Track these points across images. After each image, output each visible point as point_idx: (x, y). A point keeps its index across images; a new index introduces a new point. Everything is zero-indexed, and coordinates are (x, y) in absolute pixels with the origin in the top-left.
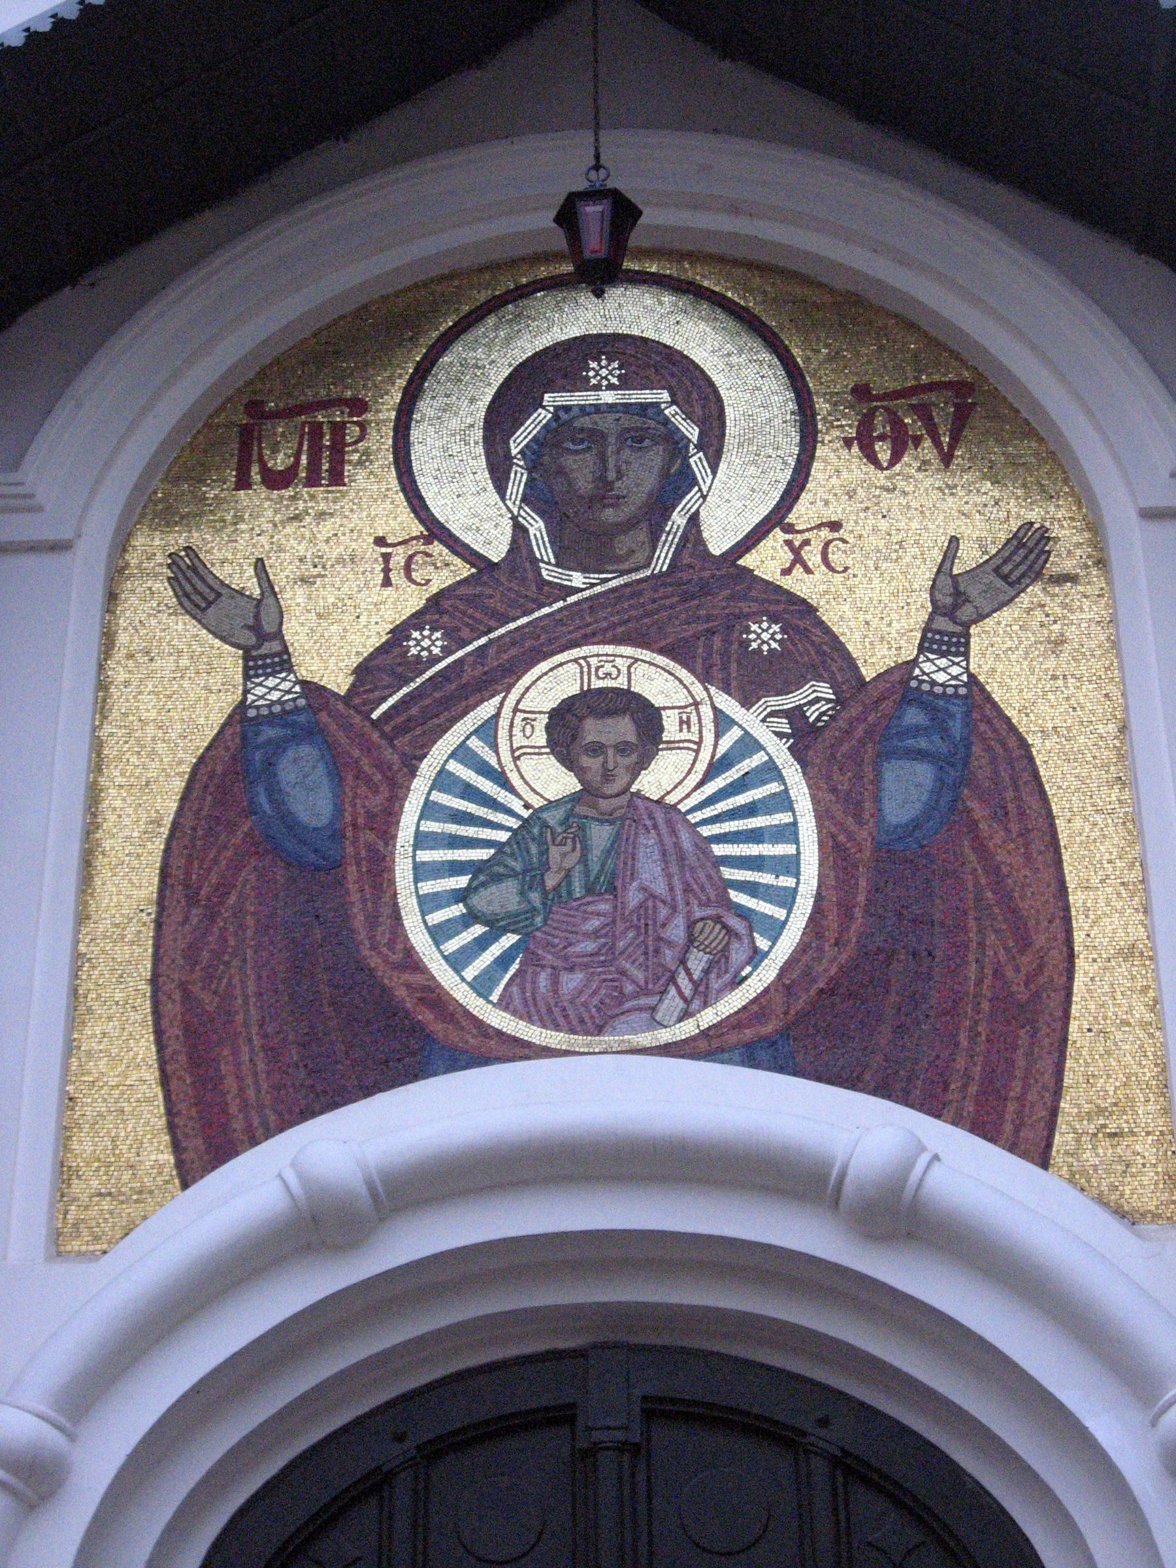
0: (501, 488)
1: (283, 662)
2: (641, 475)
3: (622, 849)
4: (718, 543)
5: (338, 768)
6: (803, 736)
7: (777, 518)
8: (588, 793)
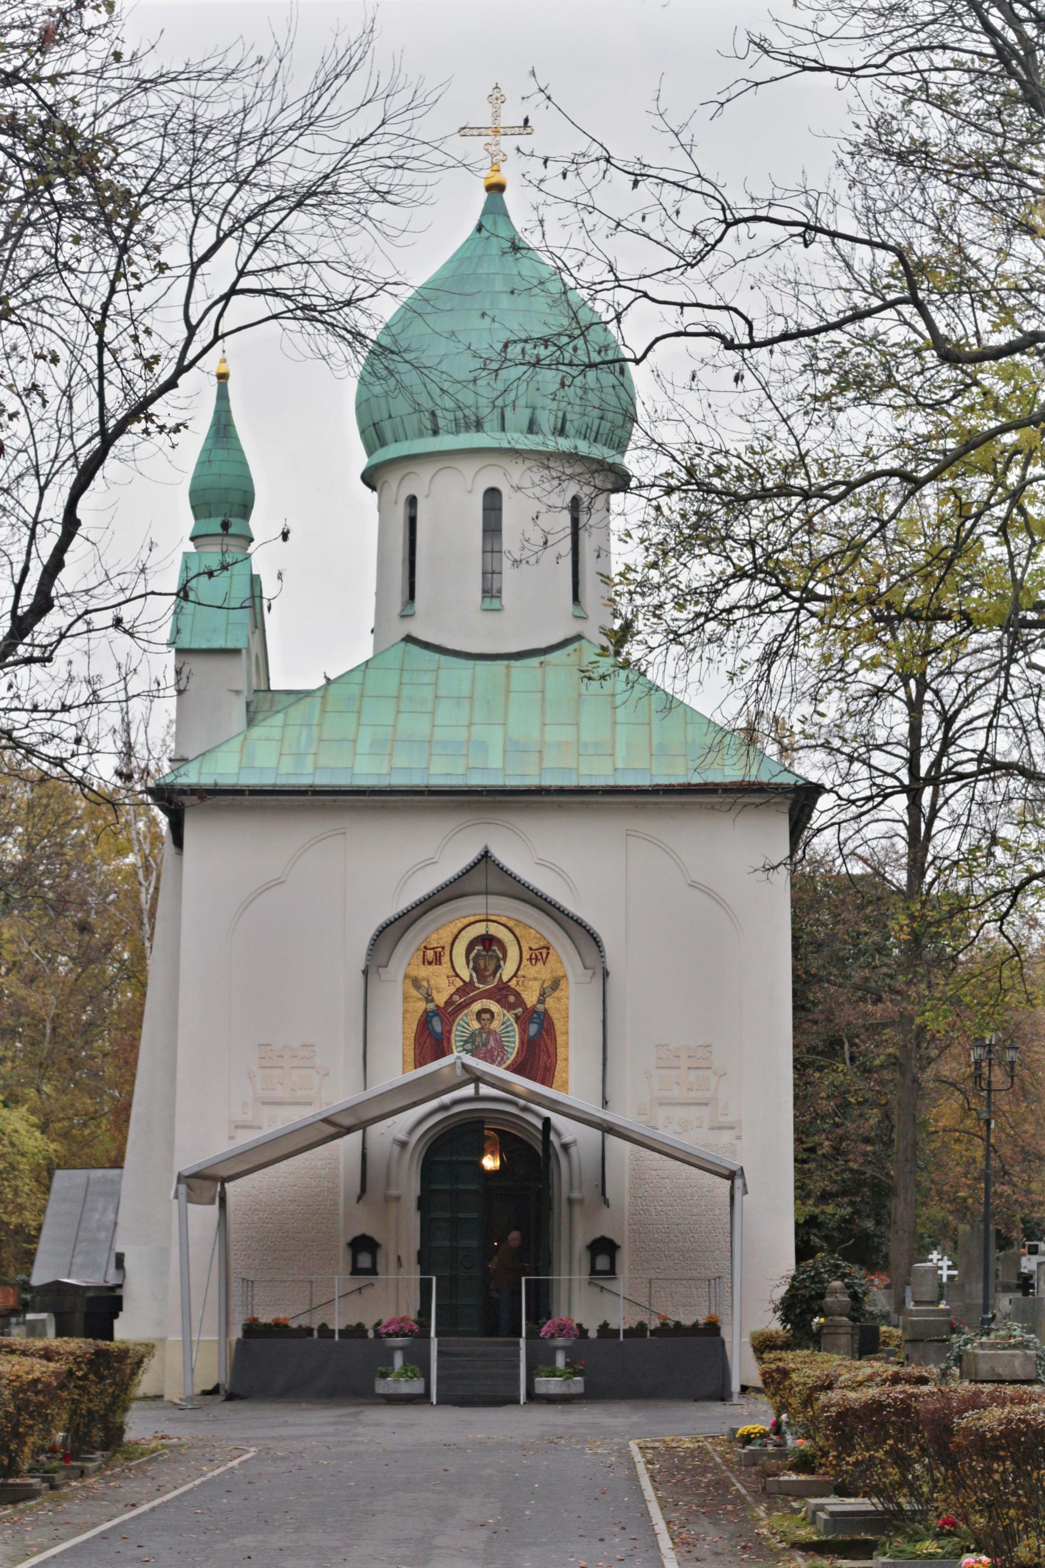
0: (468, 963)
1: (432, 1001)
2: (491, 967)
3: (488, 1038)
4: (505, 979)
5: (442, 1021)
6: (517, 1018)
7: (515, 975)
8: (482, 1028)
